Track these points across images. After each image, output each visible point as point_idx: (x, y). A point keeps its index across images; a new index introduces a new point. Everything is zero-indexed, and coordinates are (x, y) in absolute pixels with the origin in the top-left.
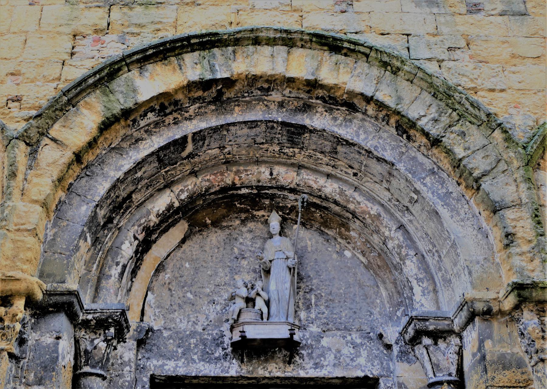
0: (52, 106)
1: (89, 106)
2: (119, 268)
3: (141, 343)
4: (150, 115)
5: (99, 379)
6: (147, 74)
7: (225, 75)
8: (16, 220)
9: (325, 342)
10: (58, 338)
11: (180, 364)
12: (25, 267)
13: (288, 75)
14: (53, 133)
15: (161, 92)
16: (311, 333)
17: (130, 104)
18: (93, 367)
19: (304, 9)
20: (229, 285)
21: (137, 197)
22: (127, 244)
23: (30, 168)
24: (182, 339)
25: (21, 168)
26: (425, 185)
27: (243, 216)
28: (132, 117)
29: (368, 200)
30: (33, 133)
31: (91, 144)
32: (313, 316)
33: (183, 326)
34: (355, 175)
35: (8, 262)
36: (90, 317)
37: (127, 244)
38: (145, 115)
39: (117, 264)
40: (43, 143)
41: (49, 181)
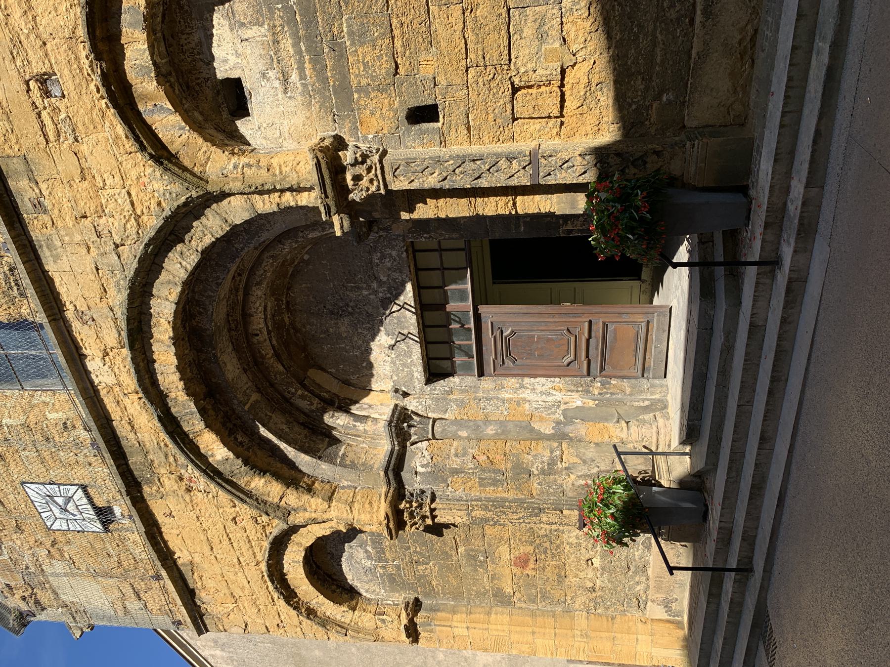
0: (256, 507)
1: (248, 483)
2: (358, 424)
3: (405, 395)
4: (240, 439)
5: (435, 428)
6: (210, 453)
7: (193, 405)
8: (345, 515)
9: (385, 279)
10: (416, 473)
11: (415, 369)
12: (376, 508)
13: (176, 362)
14: (276, 500)
15: (222, 445)
16: (378, 287)
17: (240, 461)
18: (428, 433)
19: (103, 347)
20: (351, 340)
21: (302, 418)
22: (338, 421)
23: (305, 510)
24: (396, 371)
25: (307, 515)
26: (243, 249)
27: (292, 331)
28: (246, 452)
29: (261, 264)
30: (279, 514)
31: (277, 476)
32: (365, 285)
33: (388, 368)
34: (240, 275)
35: (374, 516)
36: (396, 443)
37: (338, 421)
38: (241, 443)
39: (355, 426)
40: (285, 505)
41: (312, 500)
